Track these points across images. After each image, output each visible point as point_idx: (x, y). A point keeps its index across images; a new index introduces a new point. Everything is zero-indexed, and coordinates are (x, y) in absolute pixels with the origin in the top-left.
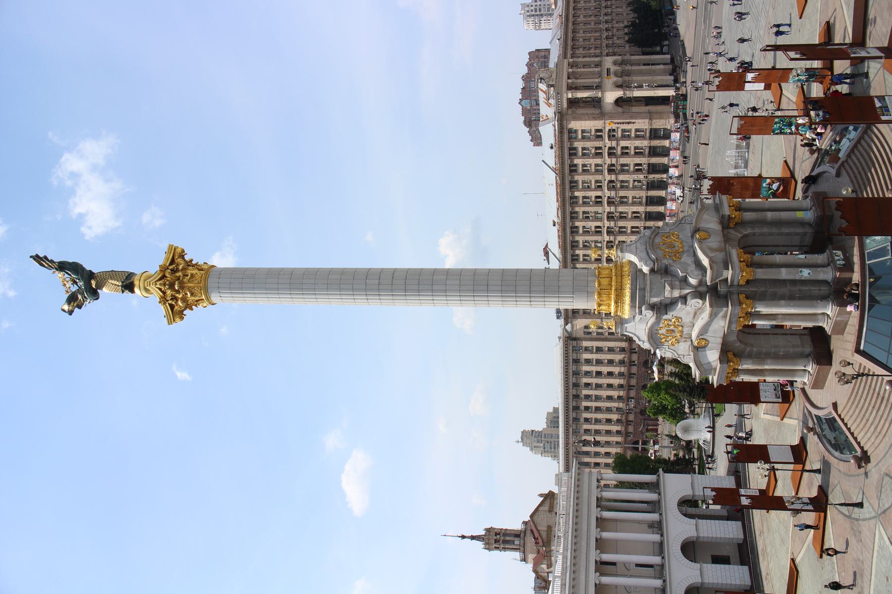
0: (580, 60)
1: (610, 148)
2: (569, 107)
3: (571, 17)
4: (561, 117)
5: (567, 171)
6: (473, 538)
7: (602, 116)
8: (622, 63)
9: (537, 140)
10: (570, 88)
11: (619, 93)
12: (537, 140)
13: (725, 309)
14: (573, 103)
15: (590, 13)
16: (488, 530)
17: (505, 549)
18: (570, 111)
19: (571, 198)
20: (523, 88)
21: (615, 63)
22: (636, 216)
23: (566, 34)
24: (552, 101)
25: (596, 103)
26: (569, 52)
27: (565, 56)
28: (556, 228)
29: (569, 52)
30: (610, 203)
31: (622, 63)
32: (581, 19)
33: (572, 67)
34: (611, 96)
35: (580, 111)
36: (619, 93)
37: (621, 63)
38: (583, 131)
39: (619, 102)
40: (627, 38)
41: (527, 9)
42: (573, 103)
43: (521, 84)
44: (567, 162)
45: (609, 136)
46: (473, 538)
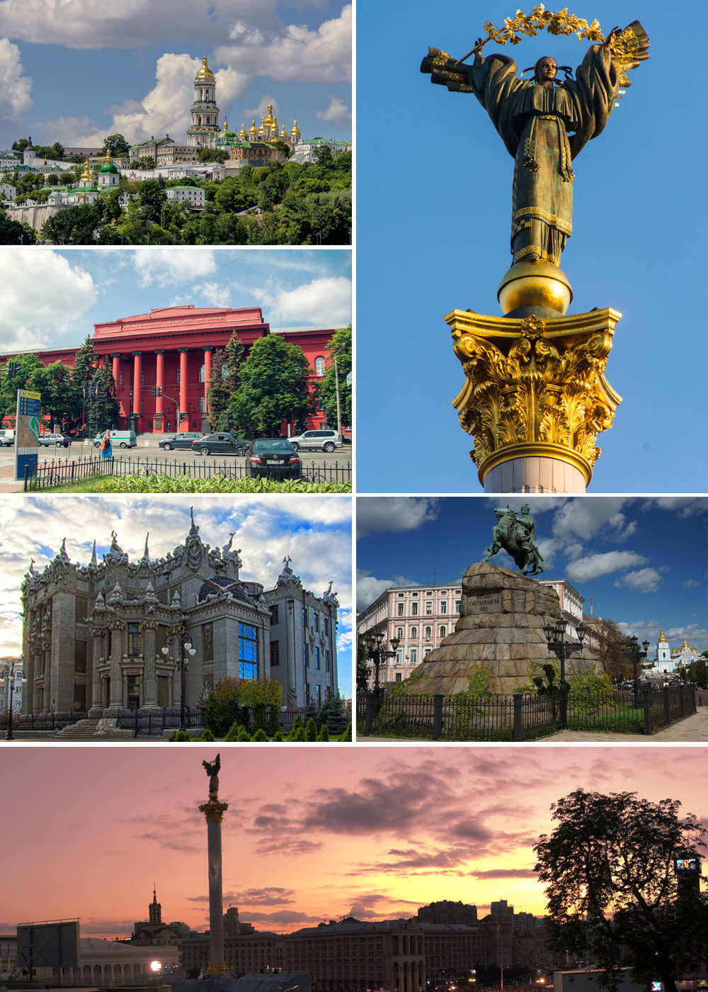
0: (424, 943)
2: (394, 937)
6: (155, 897)
8: (420, 965)
10: (404, 937)
11: (401, 965)
14: (396, 938)
16: (159, 905)
17: (150, 915)
21: (421, 962)
23: (447, 934)
25: (396, 953)
26: (428, 936)
27: (426, 933)
29: (428, 936)
33: (419, 938)
34: (401, 960)
37: (420, 965)
39: (396, 964)
46: (155, 897)
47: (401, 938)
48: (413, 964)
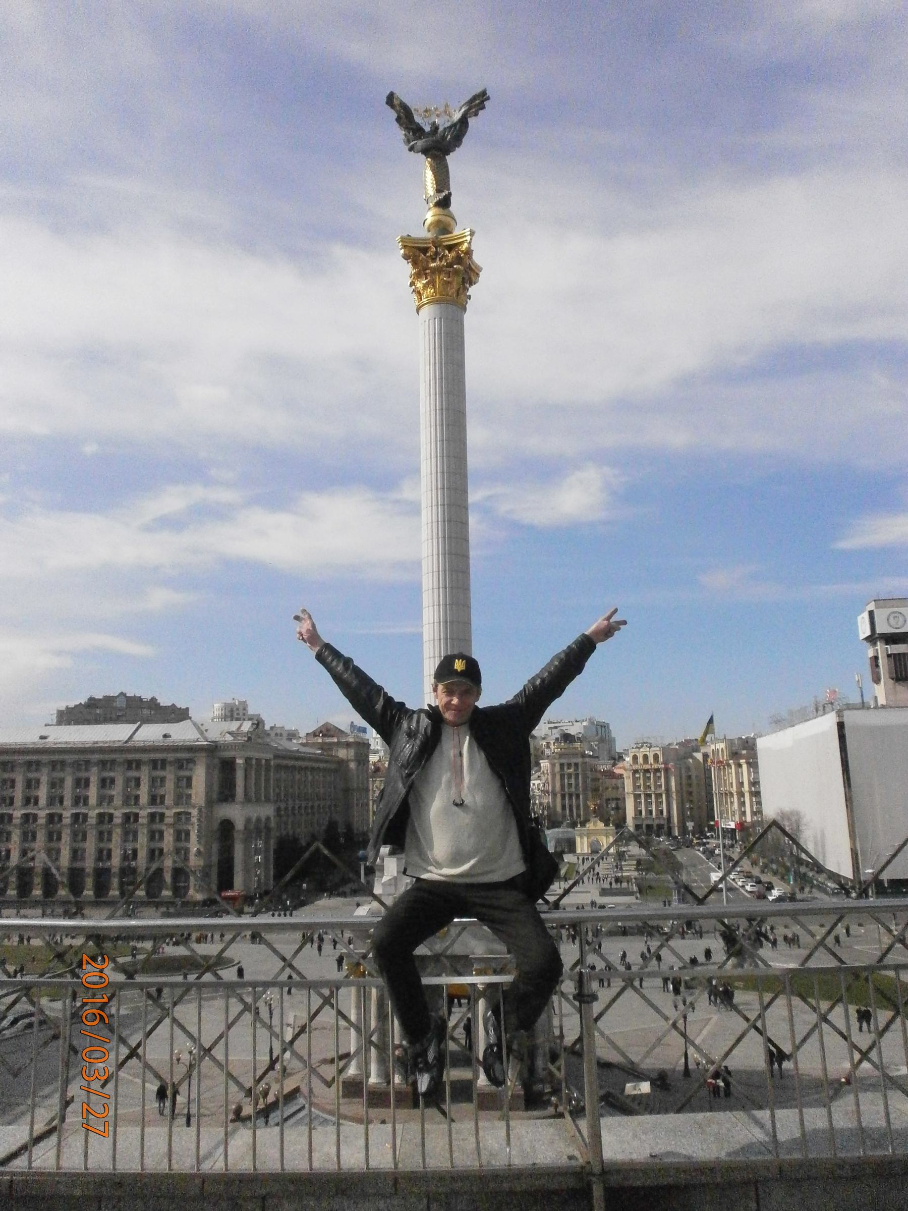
1: (162, 815)
3: (299, 763)
4: (213, 749)
5: (130, 756)
7: (210, 802)
9: (68, 717)
10: (248, 760)
12: (68, 717)
13: (505, 949)
15: (302, 787)
18: (216, 761)
19: (87, 762)
20: (140, 699)
21: (268, 819)
22: (103, 855)
24: (229, 738)
27: (276, 757)
28: (36, 739)
30: (51, 818)
31: (268, 829)
32: (297, 777)
35: (216, 773)
36: (239, 825)
38: (189, 780)
39: (227, 827)
40: (291, 832)
41: (241, 708)
42: (228, 766)
43: (146, 696)
44: (145, 757)
45: (179, 814)
47: (240, 761)
48: (258, 820)
